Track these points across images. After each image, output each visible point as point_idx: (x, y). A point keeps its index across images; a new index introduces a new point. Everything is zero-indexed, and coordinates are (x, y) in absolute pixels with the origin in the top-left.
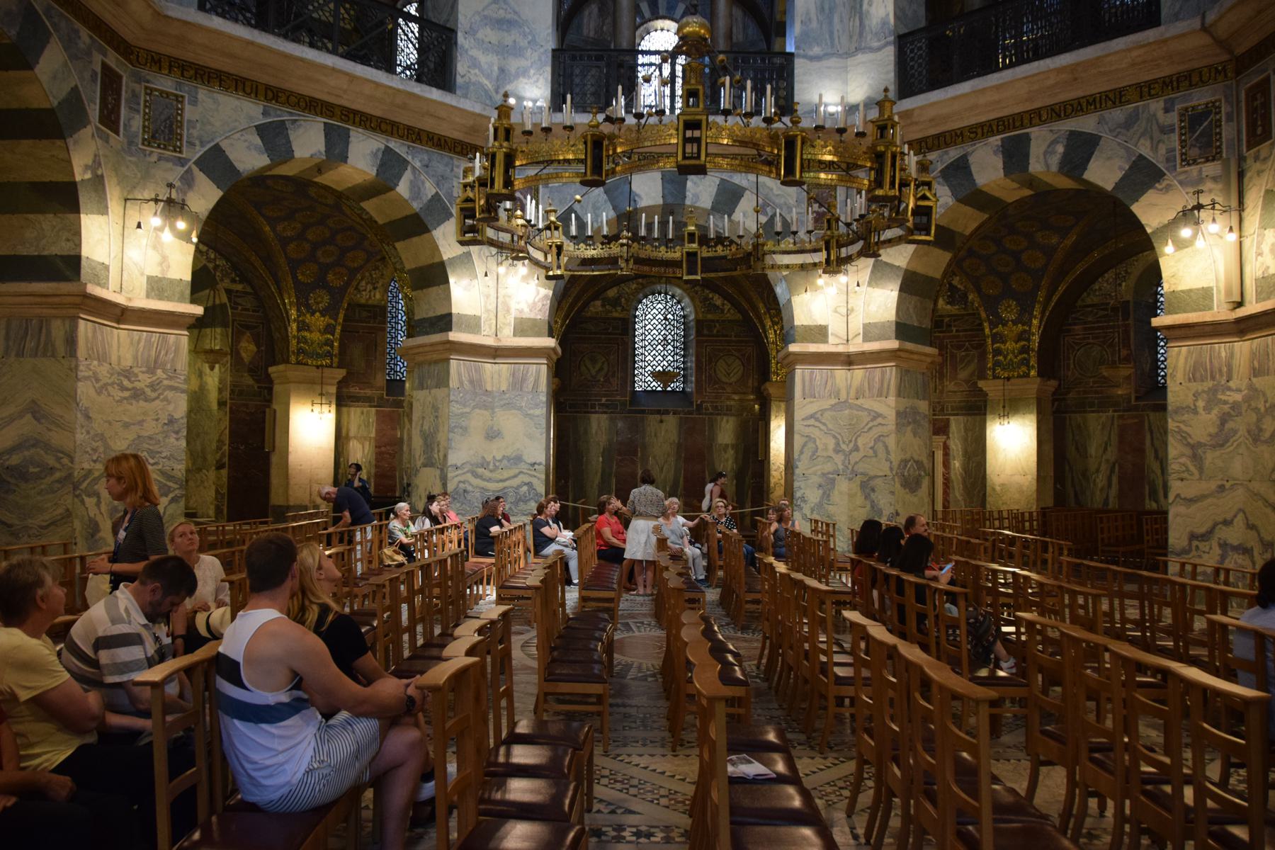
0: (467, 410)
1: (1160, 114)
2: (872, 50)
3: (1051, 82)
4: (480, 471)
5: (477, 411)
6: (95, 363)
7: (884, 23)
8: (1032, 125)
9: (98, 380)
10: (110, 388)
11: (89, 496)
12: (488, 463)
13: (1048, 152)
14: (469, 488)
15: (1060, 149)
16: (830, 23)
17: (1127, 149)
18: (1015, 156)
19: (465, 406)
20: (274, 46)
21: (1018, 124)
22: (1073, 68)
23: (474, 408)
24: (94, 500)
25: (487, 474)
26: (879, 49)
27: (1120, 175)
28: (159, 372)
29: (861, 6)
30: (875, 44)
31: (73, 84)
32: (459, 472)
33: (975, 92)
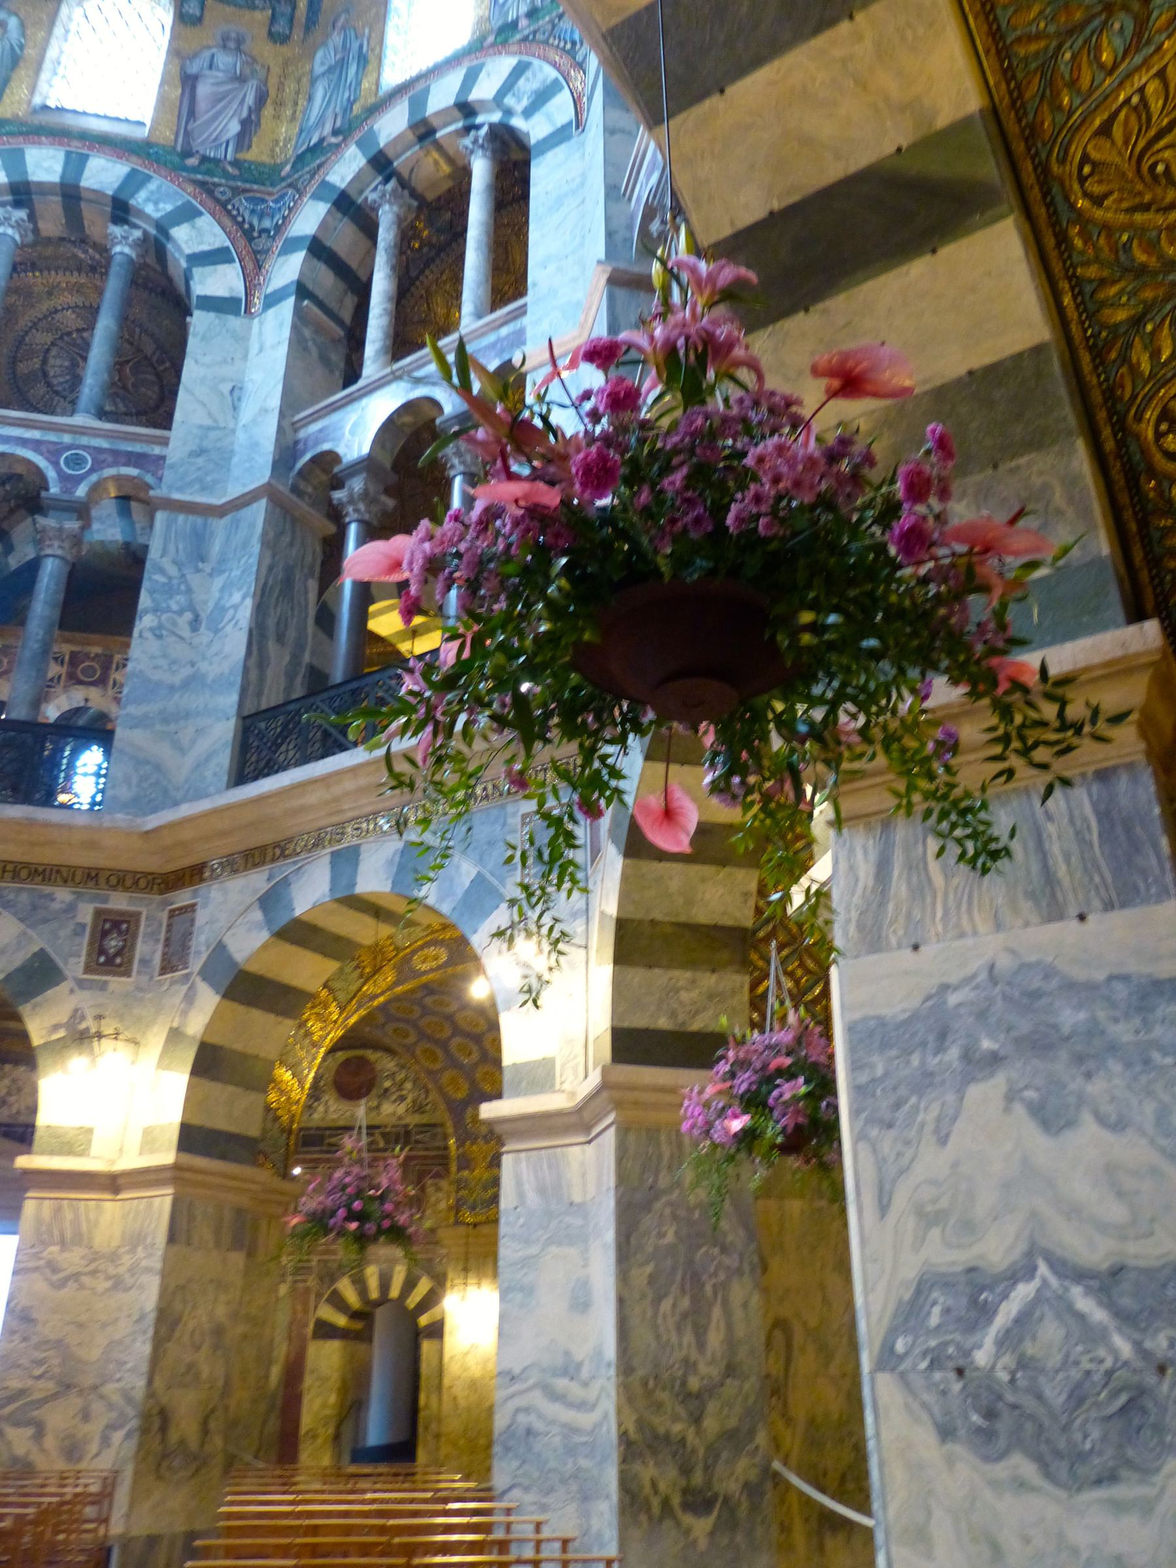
0: (534, 1250)
4: (562, 1383)
5: (554, 1249)
6: (55, 1249)
9: (55, 1270)
10: (86, 1280)
11: (17, 1424)
12: (579, 1366)
14: (539, 1425)
19: (528, 1242)
20: (233, 800)
23: (550, 1241)
24: (30, 1431)
25: (575, 1390)
28: (140, 1249)
31: (36, 949)
32: (517, 1387)
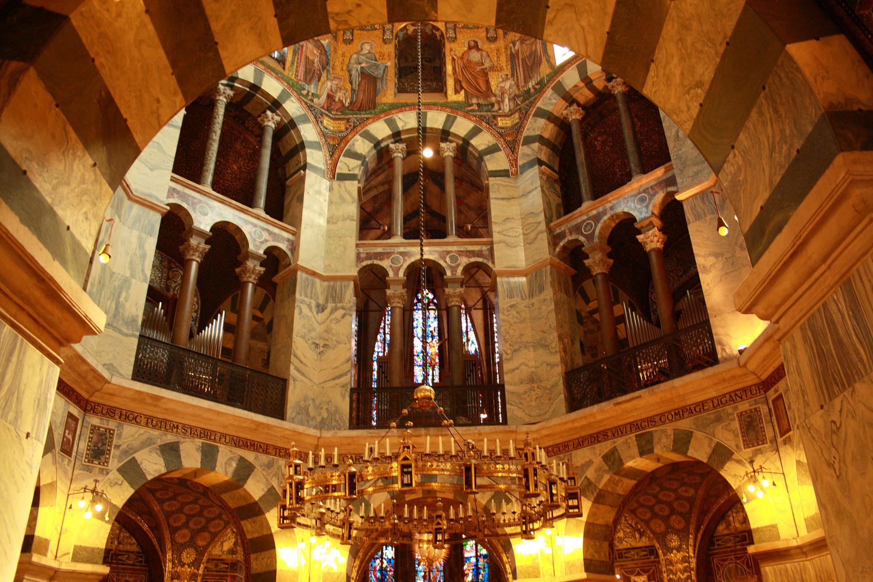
1: (283, 467)
2: (121, 332)
3: (245, 425)
7: (134, 320)
8: (220, 442)
13: (227, 464)
15: (234, 465)
16: (101, 294)
17: (267, 480)
18: (209, 456)
21: (213, 437)
22: (259, 424)
26: (127, 335)
27: (262, 493)
29: (119, 296)
30: (125, 330)
33: (209, 410)
